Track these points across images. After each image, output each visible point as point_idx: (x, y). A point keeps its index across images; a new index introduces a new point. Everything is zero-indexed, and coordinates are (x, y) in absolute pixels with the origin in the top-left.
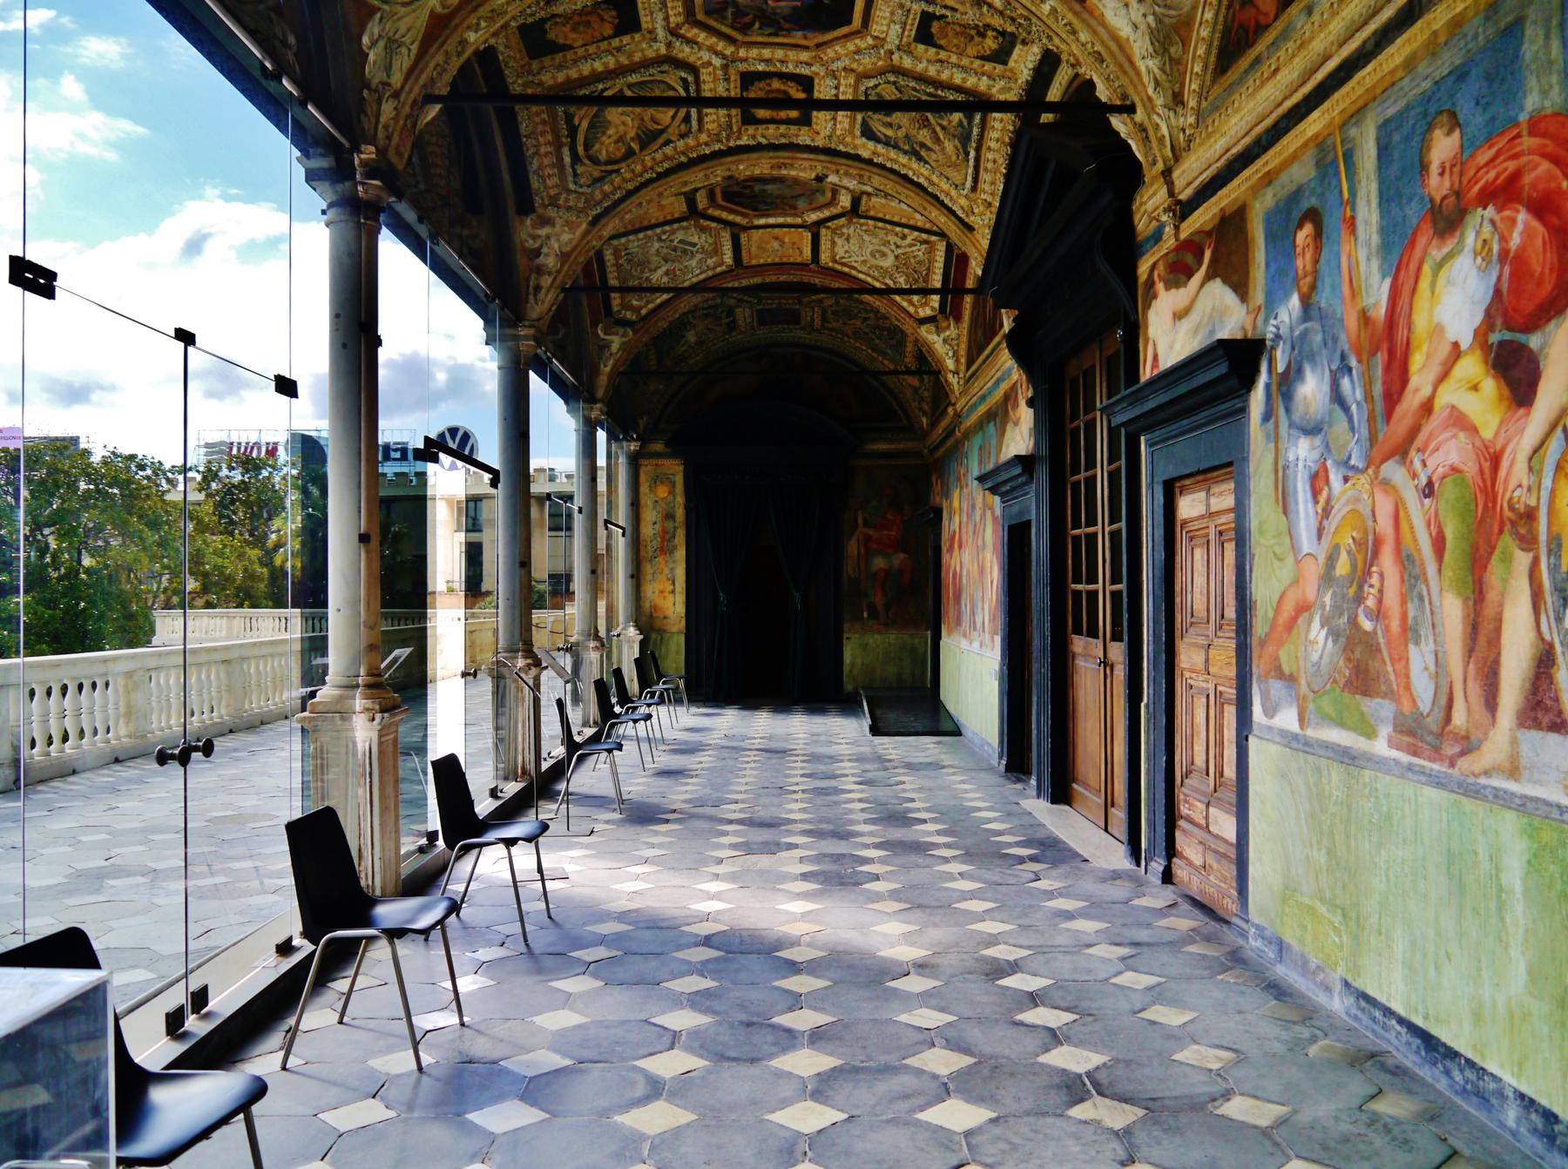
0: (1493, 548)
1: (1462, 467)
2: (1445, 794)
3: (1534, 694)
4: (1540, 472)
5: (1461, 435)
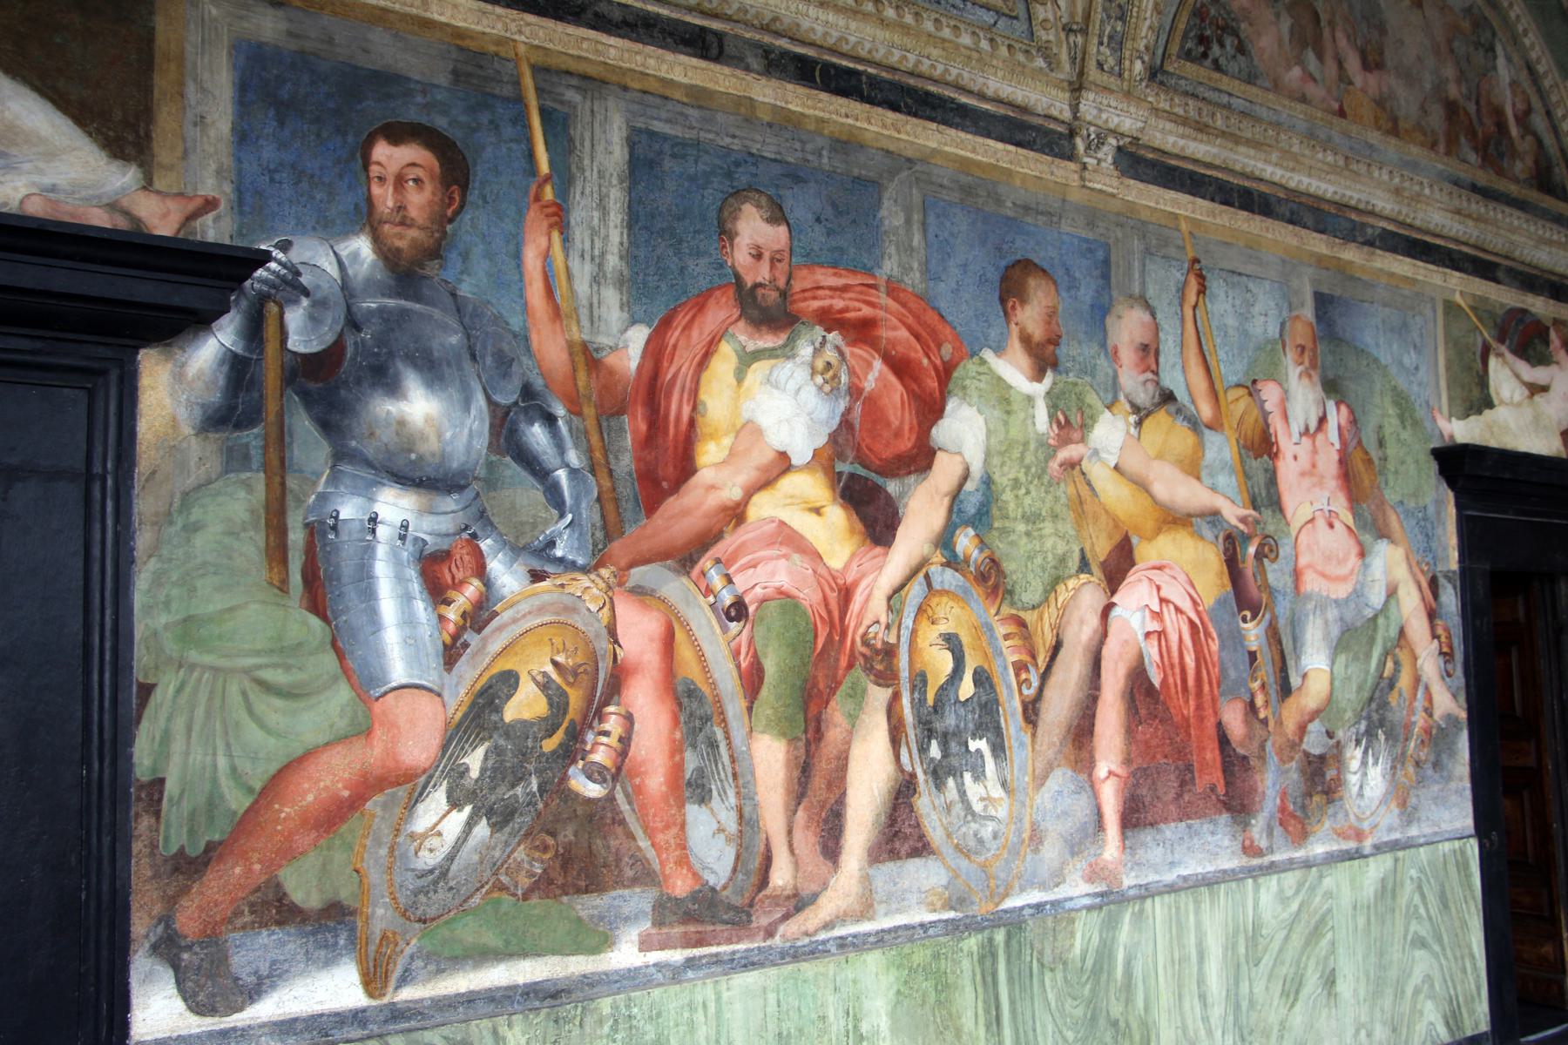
0: (839, 683)
1: (794, 592)
2: (772, 972)
3: (891, 825)
4: (900, 612)
5: (796, 557)
